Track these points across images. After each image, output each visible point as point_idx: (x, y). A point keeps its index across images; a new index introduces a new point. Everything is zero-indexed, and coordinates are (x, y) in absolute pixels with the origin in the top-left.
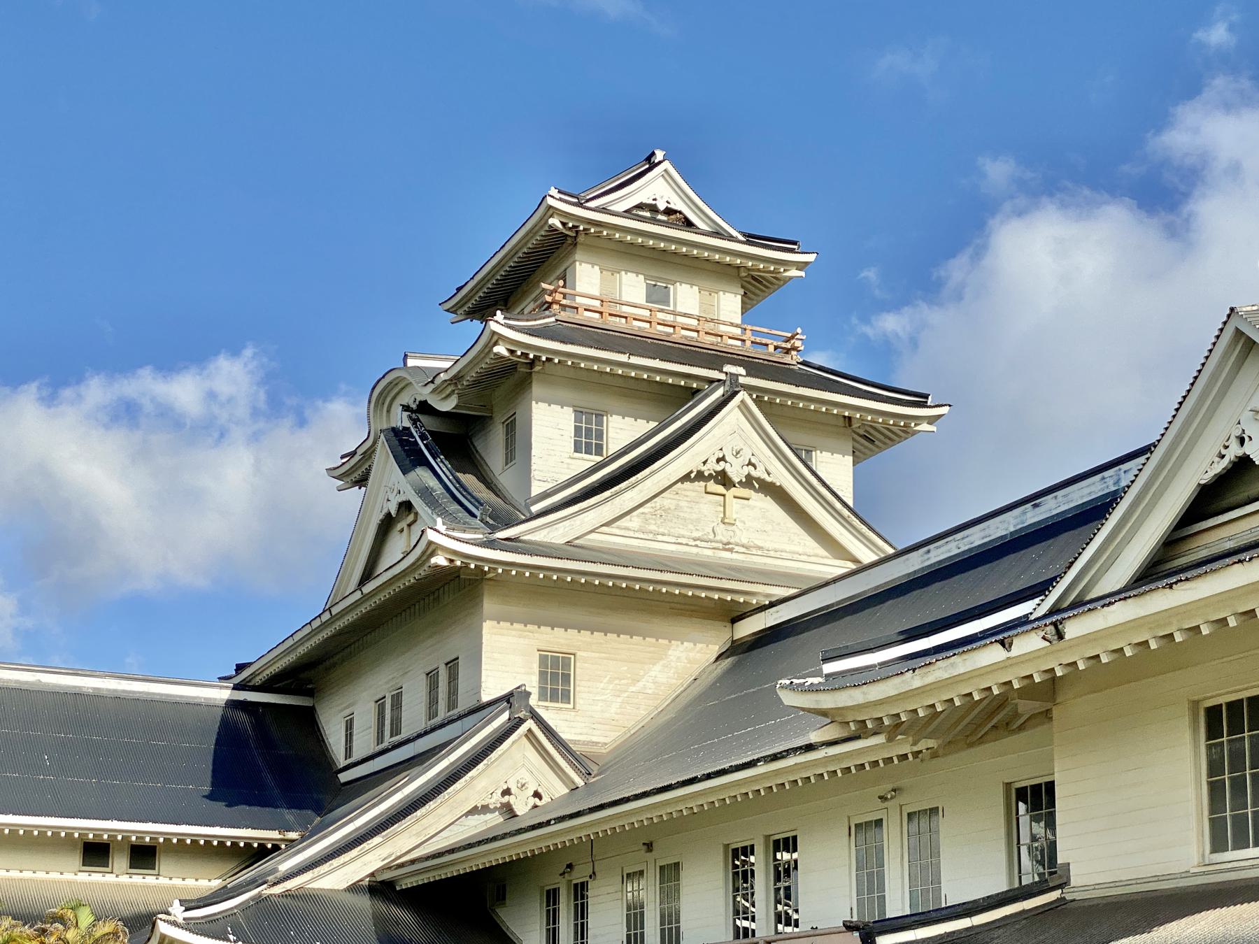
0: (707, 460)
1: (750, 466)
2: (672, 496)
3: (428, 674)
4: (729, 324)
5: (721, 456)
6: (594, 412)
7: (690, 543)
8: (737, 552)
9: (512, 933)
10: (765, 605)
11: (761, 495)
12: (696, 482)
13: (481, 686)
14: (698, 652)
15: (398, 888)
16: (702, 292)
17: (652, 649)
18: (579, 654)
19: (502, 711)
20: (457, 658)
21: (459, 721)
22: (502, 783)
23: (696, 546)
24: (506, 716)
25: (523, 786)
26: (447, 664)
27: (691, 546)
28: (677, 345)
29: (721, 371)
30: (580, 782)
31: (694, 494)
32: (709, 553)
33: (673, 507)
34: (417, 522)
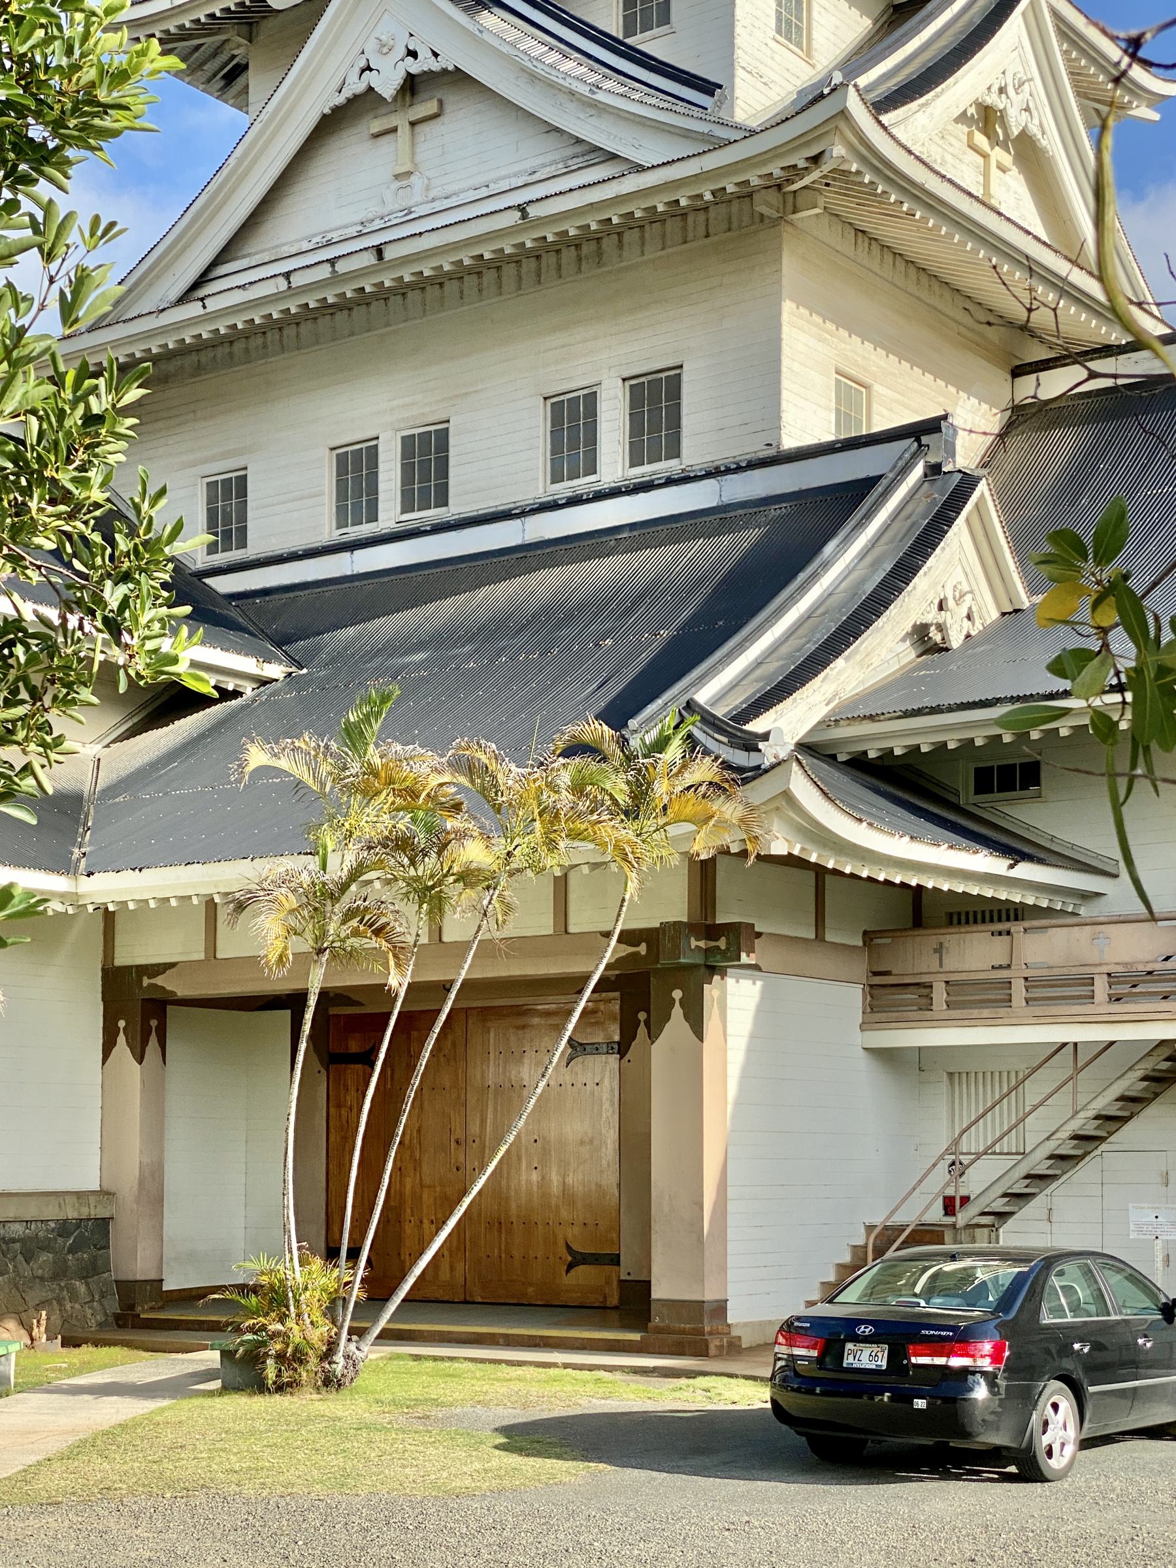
3: (545, 399)
9: (1053, 838)
10: (1118, 346)
13: (780, 418)
14: (983, 416)
15: (842, 758)
17: (941, 399)
18: (877, 388)
19: (915, 456)
20: (681, 367)
21: (712, 481)
22: (939, 588)
24: (918, 471)
25: (961, 597)
26: (624, 380)
30: (1025, 601)
34: (439, 120)
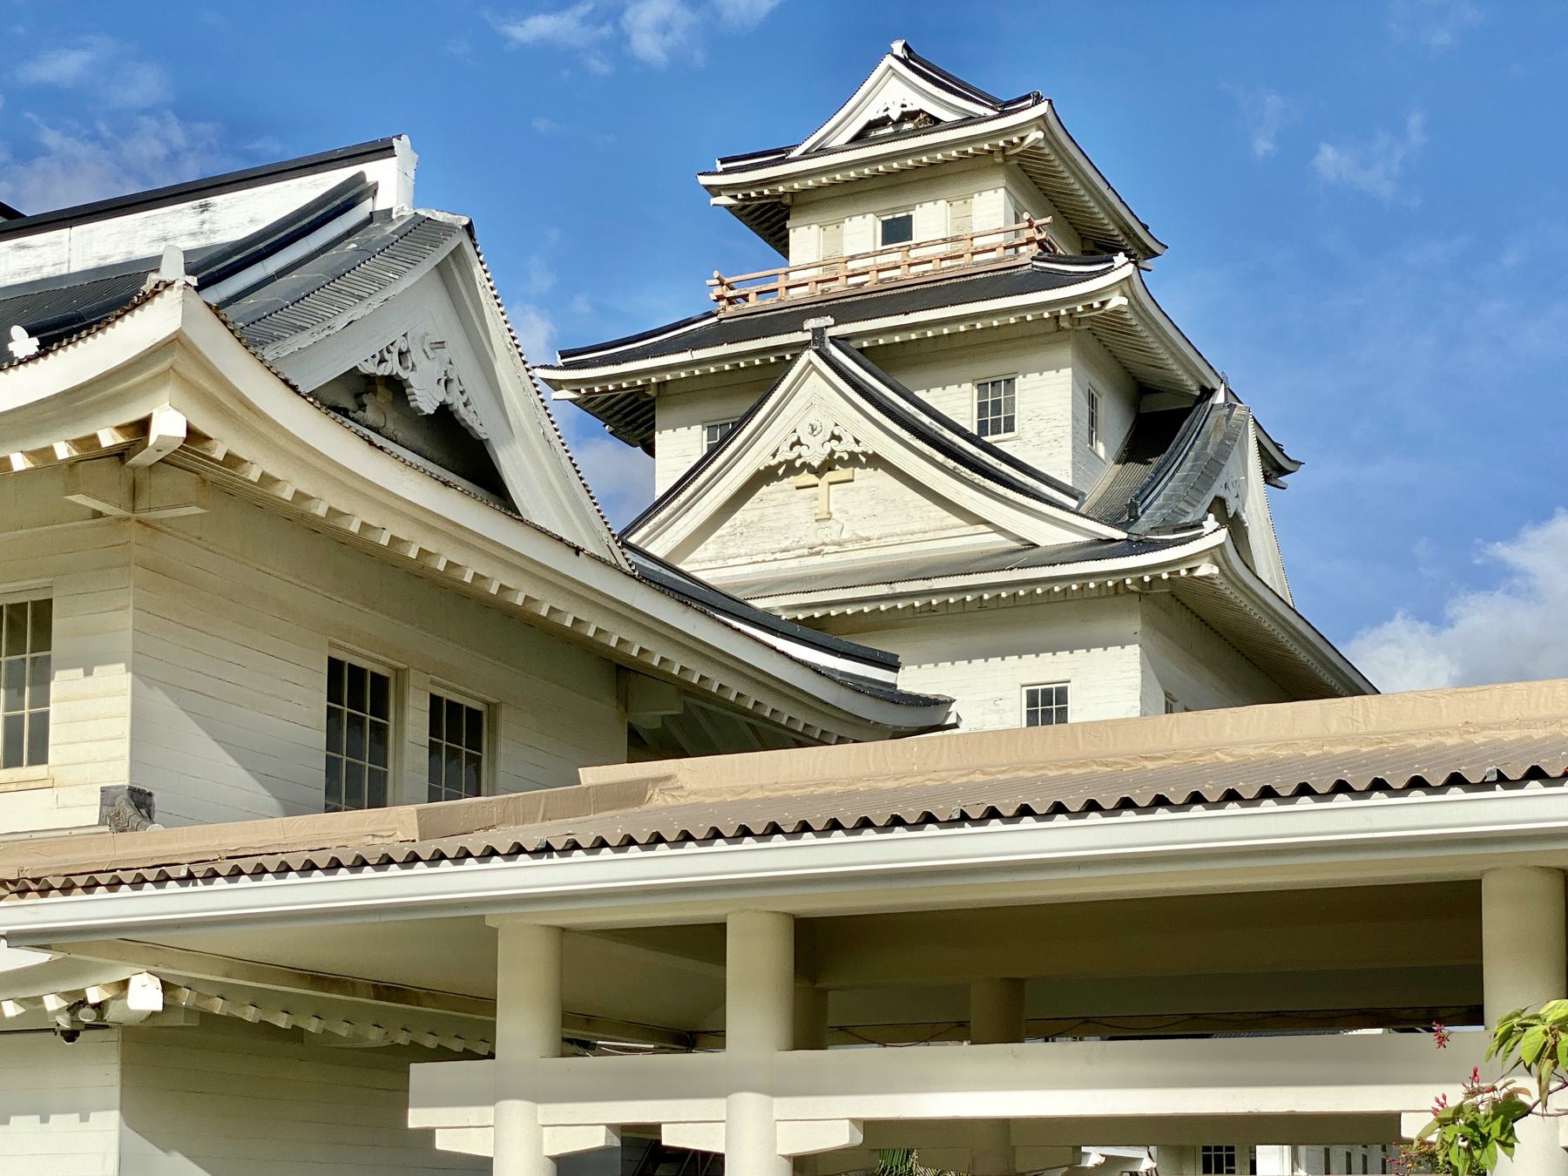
0: (777, 450)
1: (833, 441)
2: (755, 506)
4: (941, 241)
5: (794, 439)
6: (718, 423)
7: (767, 559)
8: (827, 553)
11: (870, 471)
12: (786, 479)
16: (954, 203)
23: (775, 560)
27: (770, 561)
28: (868, 296)
29: (804, 331)
31: (780, 496)
32: (794, 563)
33: (755, 519)
